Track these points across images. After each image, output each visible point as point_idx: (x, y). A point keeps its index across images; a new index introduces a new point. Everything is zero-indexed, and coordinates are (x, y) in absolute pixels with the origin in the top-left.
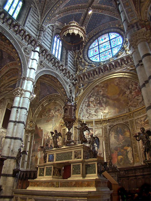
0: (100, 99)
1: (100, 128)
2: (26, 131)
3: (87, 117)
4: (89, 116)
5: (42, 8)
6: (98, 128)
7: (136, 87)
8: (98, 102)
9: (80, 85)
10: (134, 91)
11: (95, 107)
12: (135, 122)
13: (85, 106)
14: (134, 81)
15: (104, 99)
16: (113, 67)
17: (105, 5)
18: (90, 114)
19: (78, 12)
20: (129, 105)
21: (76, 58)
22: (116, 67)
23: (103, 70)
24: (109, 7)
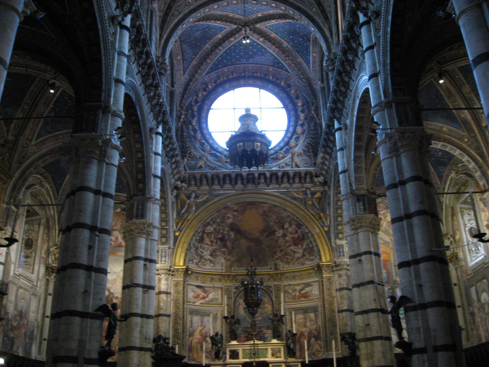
0: (224, 230)
1: (217, 288)
2: (47, 268)
3: (197, 264)
4: (200, 261)
5: (164, 8)
6: (214, 287)
7: (297, 229)
8: (220, 236)
9: (191, 194)
10: (291, 234)
11: (212, 245)
12: (284, 290)
13: (196, 240)
14: (297, 220)
15: (232, 233)
16: (266, 181)
17: (276, 35)
18: (201, 257)
19: (219, 24)
20: (276, 257)
21: (182, 121)
22: (271, 182)
23: (245, 181)
24: (284, 41)
